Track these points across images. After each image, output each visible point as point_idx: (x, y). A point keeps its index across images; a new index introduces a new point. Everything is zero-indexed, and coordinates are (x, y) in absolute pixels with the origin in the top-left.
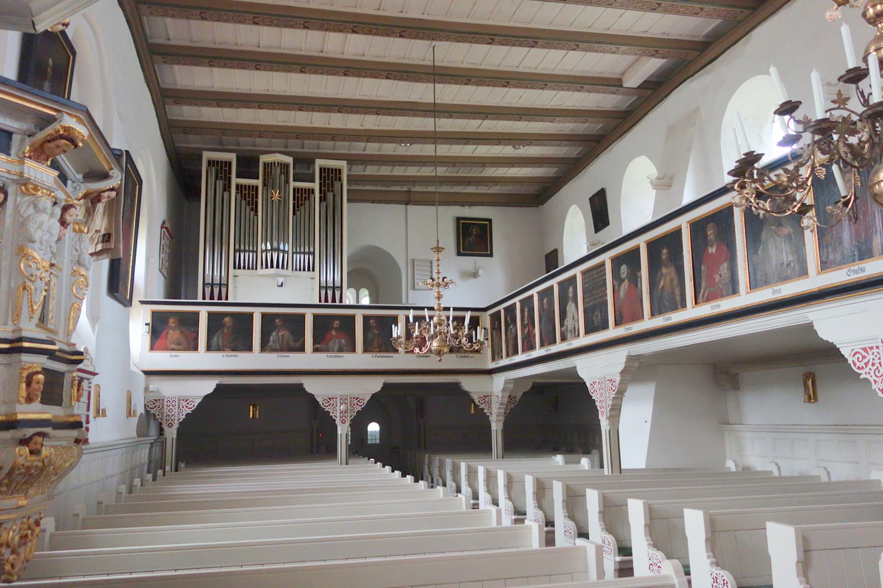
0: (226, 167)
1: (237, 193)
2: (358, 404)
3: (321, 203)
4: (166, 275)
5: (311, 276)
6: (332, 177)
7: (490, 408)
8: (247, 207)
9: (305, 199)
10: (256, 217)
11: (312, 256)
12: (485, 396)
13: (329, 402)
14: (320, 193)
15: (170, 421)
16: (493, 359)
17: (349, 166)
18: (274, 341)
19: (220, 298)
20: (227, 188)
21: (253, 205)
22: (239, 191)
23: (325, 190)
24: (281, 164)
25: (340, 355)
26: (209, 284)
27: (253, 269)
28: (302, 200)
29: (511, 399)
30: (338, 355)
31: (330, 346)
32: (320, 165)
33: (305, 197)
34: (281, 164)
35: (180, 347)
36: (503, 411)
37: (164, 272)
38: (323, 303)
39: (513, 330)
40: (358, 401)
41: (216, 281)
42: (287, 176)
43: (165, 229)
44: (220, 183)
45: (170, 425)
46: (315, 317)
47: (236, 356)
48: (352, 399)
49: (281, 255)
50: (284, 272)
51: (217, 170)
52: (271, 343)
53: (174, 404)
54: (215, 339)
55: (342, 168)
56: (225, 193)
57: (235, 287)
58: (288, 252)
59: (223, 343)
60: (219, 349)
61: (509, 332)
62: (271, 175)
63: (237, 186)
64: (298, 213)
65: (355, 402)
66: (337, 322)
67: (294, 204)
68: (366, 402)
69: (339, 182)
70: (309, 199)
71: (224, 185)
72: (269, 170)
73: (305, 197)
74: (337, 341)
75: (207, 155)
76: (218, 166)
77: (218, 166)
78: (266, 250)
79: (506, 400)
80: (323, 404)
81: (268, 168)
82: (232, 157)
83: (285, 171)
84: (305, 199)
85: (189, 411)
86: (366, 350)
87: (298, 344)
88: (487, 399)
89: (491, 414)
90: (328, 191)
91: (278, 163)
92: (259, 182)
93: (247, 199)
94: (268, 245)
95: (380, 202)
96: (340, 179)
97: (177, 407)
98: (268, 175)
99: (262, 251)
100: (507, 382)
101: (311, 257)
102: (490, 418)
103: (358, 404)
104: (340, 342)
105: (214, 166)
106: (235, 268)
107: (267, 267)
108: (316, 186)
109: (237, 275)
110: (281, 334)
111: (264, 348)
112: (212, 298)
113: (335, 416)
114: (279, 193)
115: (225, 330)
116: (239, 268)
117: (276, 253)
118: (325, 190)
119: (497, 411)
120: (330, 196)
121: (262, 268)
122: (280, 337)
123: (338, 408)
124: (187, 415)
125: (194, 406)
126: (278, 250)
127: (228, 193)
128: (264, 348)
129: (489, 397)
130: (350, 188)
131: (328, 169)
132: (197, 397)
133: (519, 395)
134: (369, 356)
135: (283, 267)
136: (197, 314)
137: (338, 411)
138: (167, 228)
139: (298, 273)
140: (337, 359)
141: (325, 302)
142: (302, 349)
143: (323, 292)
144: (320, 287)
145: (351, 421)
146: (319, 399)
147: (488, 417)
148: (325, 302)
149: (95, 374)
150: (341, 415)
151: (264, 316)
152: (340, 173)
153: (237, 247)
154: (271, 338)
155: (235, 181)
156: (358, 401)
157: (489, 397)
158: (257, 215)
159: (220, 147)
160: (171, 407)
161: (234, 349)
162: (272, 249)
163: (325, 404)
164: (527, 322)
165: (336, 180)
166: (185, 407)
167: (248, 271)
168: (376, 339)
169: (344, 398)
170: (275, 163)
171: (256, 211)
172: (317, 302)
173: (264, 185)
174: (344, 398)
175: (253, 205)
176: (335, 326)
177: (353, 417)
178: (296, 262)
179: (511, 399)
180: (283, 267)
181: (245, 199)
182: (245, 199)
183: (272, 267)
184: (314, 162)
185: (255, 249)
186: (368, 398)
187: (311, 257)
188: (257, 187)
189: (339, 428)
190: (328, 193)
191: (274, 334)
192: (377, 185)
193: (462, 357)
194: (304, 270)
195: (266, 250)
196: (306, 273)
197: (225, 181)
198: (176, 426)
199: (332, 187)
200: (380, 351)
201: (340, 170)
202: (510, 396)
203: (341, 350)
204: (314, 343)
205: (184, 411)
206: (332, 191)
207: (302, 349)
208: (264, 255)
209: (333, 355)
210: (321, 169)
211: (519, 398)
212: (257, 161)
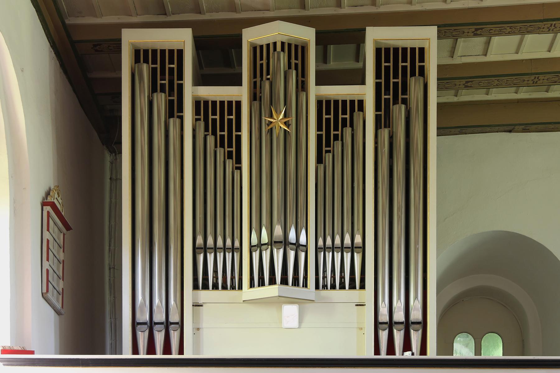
0: (171, 62)
1: (197, 120)
3: (379, 131)
4: (59, 306)
5: (357, 301)
6: (404, 68)
8: (218, 149)
9: (344, 125)
10: (237, 173)
11: (360, 255)
14: (378, 107)
17: (448, 42)
19: (167, 349)
21: (230, 146)
22: (202, 117)
23: (387, 101)
24: (290, 45)
26: (145, 323)
27: (233, 288)
28: (336, 129)
32: (376, 42)
33: (344, 120)
34: (290, 45)
37: (54, 301)
38: (383, 355)
41: (159, 317)
43: (48, 208)
44: (160, 100)
49: (291, 255)
50: (298, 292)
51: (154, 70)
55: (426, 47)
56: (171, 120)
57: (198, 329)
58: (306, 246)
62: (268, 74)
63: (197, 104)
64: (328, 158)
67: (319, 138)
69: (421, 79)
70: (352, 125)
71: (171, 103)
72: (264, 62)
73: (344, 120)
76: (154, 62)
77: (154, 62)
78: (260, 245)
81: (261, 59)
83: (299, 62)
90: (395, 102)
91: (283, 44)
93: (219, 133)
95: (527, 128)
96: (422, 72)
99: (252, 248)
101: (358, 258)
105: (146, 61)
106: (196, 287)
109: (201, 302)
112: (151, 349)
114: (285, 116)
116: (205, 287)
117: (281, 251)
118: (387, 101)
121: (252, 285)
126: (285, 243)
127: (178, 121)
131: (396, 50)
135: (296, 282)
138: (53, 205)
141: (388, 354)
143: (384, 336)
144: (377, 324)
148: (388, 354)
152: (422, 59)
153: (200, 240)
158: (240, 169)
159: (162, 18)
162: (272, 243)
165: (413, 74)
167: (225, 292)
170: (275, 44)
171: (239, 160)
172: (369, 354)
173: (255, 96)
175: (230, 146)
178: (325, 271)
180: (296, 282)
182: (214, 133)
183: (272, 281)
184: (362, 39)
185: (237, 244)
187: (358, 258)
188: (239, 104)
190: (396, 107)
192: (517, 86)
195: (260, 245)
196: (347, 294)
197: (171, 93)
199: (405, 91)
201: (422, 50)
206: (404, 101)
208: (256, 256)
210: (378, 51)
212: (237, 42)
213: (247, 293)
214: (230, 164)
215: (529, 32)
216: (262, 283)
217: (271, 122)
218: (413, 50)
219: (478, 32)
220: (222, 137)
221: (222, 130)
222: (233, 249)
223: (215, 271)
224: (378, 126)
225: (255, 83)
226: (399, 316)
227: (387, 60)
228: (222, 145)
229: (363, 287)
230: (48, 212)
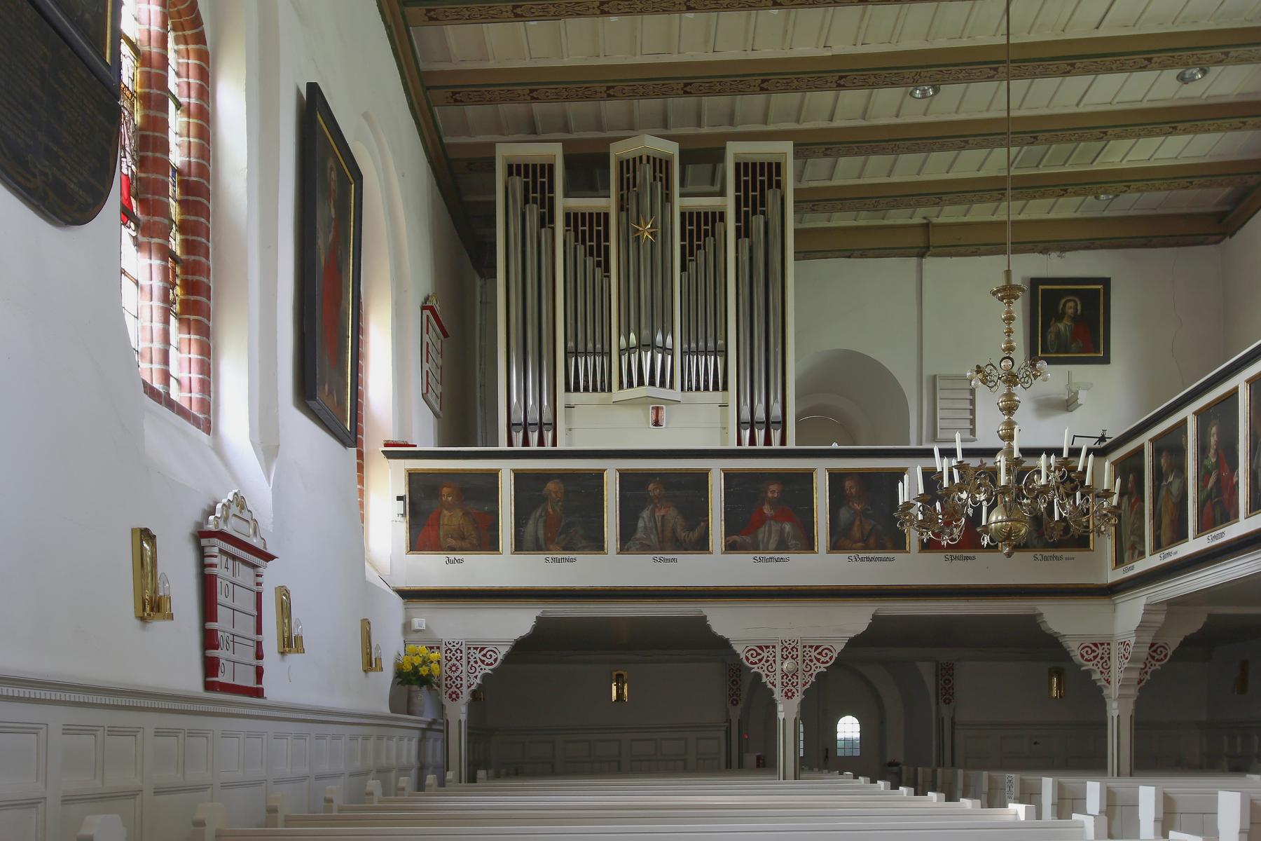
1: (567, 230)
2: (818, 660)
4: (438, 409)
6: (762, 182)
7: (1106, 669)
8: (588, 258)
9: (706, 234)
11: (723, 358)
12: (1095, 645)
13: (758, 654)
14: (738, 220)
15: (454, 689)
16: (1119, 561)
17: (801, 161)
18: (645, 527)
20: (547, 220)
22: (572, 228)
23: (746, 213)
24: (654, 159)
25: (780, 556)
26: (520, 424)
27: (603, 390)
28: (699, 239)
29: (1155, 651)
30: (777, 556)
31: (760, 537)
32: (736, 155)
33: (706, 231)
34: (654, 159)
35: (464, 544)
36: (1135, 675)
37: (433, 402)
39: (1175, 489)
40: (820, 654)
42: (668, 186)
43: (428, 312)
44: (533, 212)
45: (454, 696)
46: (729, 476)
47: (572, 560)
48: (807, 649)
51: (526, 184)
52: (639, 534)
53: (459, 655)
54: (530, 527)
55: (783, 162)
56: (543, 230)
57: (570, 430)
59: (545, 534)
60: (538, 547)
61: (1163, 492)
62: (634, 186)
64: (692, 266)
65: (814, 654)
66: (774, 487)
67: (683, 247)
68: (835, 655)
70: (713, 235)
72: (631, 175)
73: (706, 231)
74: (775, 527)
75: (506, 152)
77: (526, 176)
79: (1144, 651)
80: (747, 659)
81: (628, 172)
82: (553, 152)
83: (663, 175)
84: (706, 234)
85: (488, 670)
86: (835, 547)
87: (695, 535)
88: (1100, 651)
89: (1109, 683)
90: (754, 213)
91: (648, 157)
92: (607, 203)
93: (588, 244)
94: (632, 336)
96: (779, 185)
97: (464, 661)
98: (628, 188)
99: (621, 352)
100: (1149, 609)
102: (1105, 692)
103: (818, 660)
104: (782, 531)
105: (519, 174)
106: (567, 389)
107: (630, 385)
108: (728, 203)
110: (658, 514)
111: (628, 542)
115: (550, 510)
116: (577, 389)
118: (746, 213)
119: (1122, 676)
120: (757, 222)
121: (621, 386)
122: (658, 519)
123: (778, 667)
124: (485, 677)
125: (496, 660)
127: (550, 230)
128: (628, 542)
129: (1106, 646)
130: (800, 226)
131: (754, 165)
132: (502, 643)
133: (1174, 643)
134: (841, 558)
136: (493, 476)
137: (778, 672)
138: (432, 309)
139: (694, 394)
140: (773, 564)
142: (701, 545)
145: (804, 693)
146: (739, 649)
147: (1100, 690)
149: (269, 557)
150: (785, 681)
151: (626, 478)
152: (778, 174)
154: (641, 524)
155: (562, 203)
156: (820, 654)
157: (1106, 646)
158: (609, 277)
160: (454, 661)
161: (569, 547)
163: (751, 659)
164: (1214, 460)
165: (770, 187)
166: (480, 663)
168: (857, 523)
170: (641, 157)
171: (607, 269)
173: (622, 208)
175: (599, 255)
176: (770, 495)
177: (808, 686)
179: (1155, 651)
180: (663, 384)
181: (584, 242)
182: (584, 242)
188: (607, 215)
189: (780, 708)
191: (646, 514)
193: (1046, 559)
194: (706, 388)
197: (542, 206)
198: (465, 697)
199: (763, 205)
200: (866, 548)
201: (778, 165)
202: (1152, 645)
203: (783, 546)
204: (728, 533)
205: (478, 669)
207: (701, 545)
208: (624, 359)
209: (768, 556)
210: (737, 166)
211: (1173, 648)
212: (605, 158)
213: (617, 394)
214: (599, 271)
215: (875, 153)
216: (630, 385)
217: (638, 230)
218: (770, 164)
219: (828, 152)
220: (591, 247)
221: (591, 240)
222: (602, 354)
223: (586, 375)
224: (738, 236)
225: (622, 195)
226: (760, 414)
227: (746, 174)
228: (591, 254)
229: (725, 388)
230: (428, 316)
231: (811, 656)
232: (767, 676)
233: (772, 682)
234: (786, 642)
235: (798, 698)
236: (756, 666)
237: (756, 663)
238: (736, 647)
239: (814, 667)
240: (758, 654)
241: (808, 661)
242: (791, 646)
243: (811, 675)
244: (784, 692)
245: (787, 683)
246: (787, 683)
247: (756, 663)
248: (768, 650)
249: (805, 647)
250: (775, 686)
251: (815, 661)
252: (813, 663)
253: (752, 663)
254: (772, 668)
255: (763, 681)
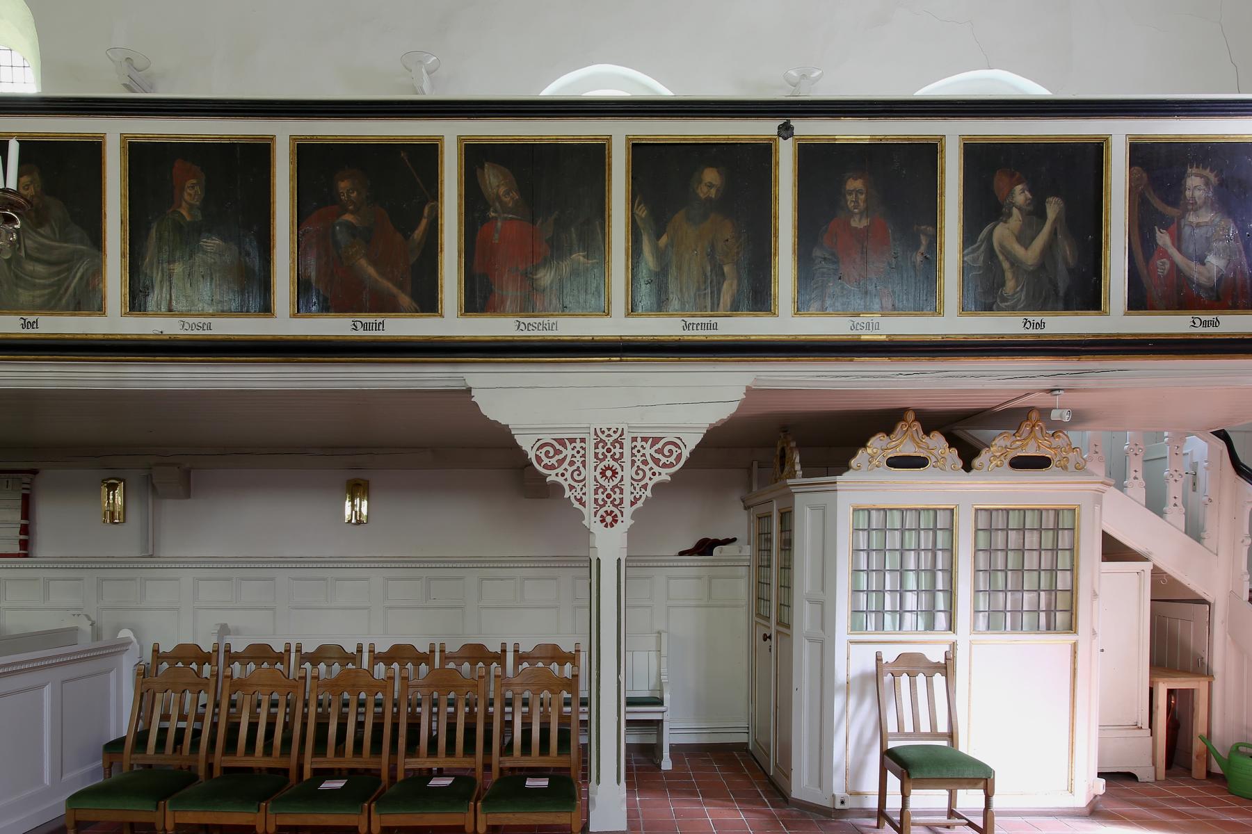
13: (557, 452)
40: (660, 451)
48: (639, 443)
65: (649, 451)
68: (686, 454)
80: (539, 459)
103: (656, 461)
113: (580, 501)
146: (526, 443)
156: (660, 451)
163: (546, 461)
169: (609, 441)
174: (609, 441)
177: (640, 504)
186: (692, 441)
231: (644, 455)
232: (571, 487)
233: (578, 497)
234: (603, 432)
235: (626, 522)
236: (553, 472)
237: (552, 467)
238: (520, 440)
239: (649, 474)
240: (557, 452)
241: (638, 463)
242: (611, 439)
243: (645, 487)
244: (599, 515)
245: (603, 500)
246: (603, 500)
247: (552, 467)
248: (573, 444)
249: (634, 439)
250: (584, 504)
251: (651, 464)
252: (649, 466)
253: (546, 467)
254: (578, 475)
255: (566, 496)
